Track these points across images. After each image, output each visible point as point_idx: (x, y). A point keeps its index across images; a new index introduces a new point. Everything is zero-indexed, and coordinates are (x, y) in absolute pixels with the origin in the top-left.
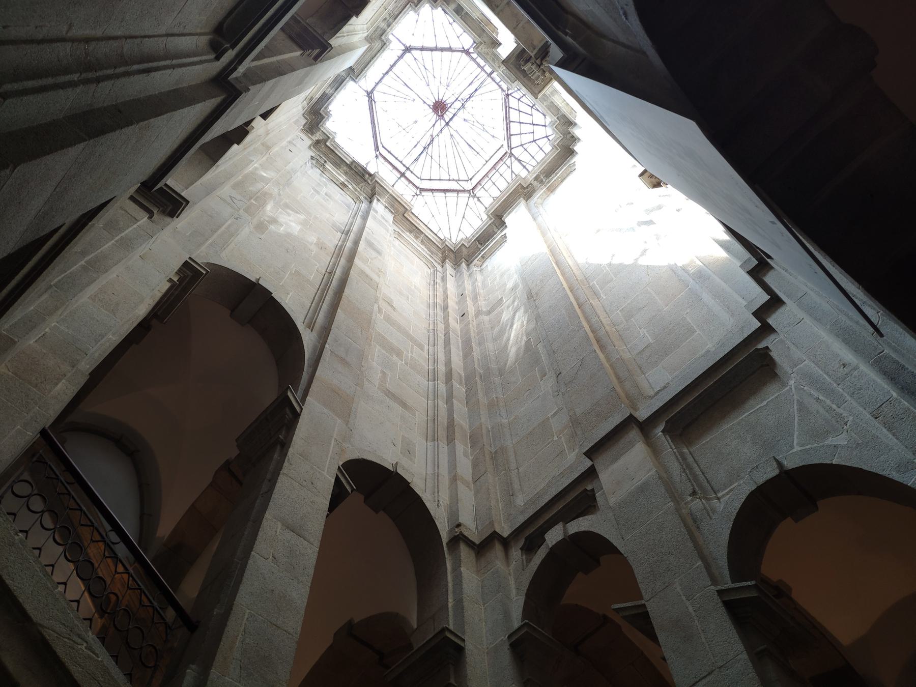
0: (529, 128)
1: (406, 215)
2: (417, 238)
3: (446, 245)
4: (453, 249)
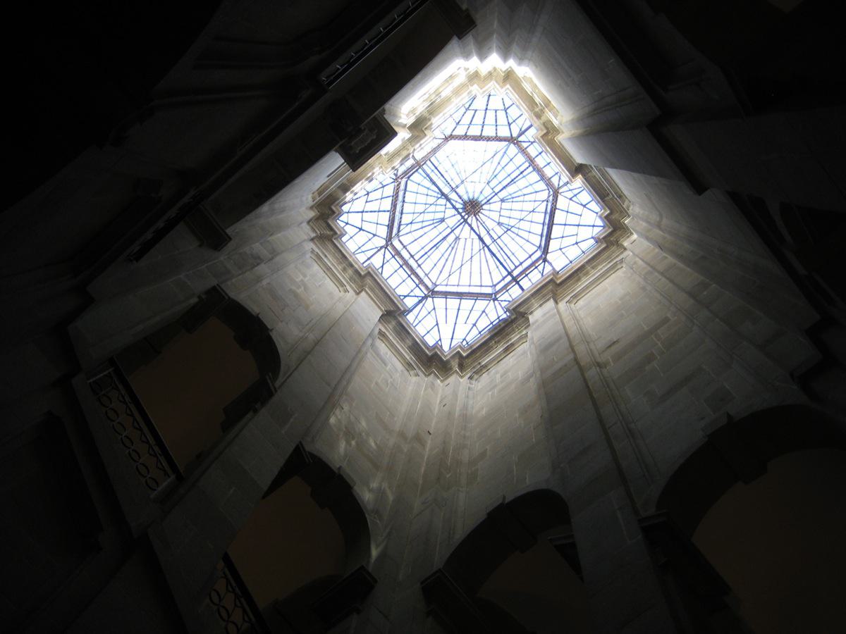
0: (491, 115)
1: (558, 282)
2: (587, 273)
3: (603, 238)
4: (610, 230)
